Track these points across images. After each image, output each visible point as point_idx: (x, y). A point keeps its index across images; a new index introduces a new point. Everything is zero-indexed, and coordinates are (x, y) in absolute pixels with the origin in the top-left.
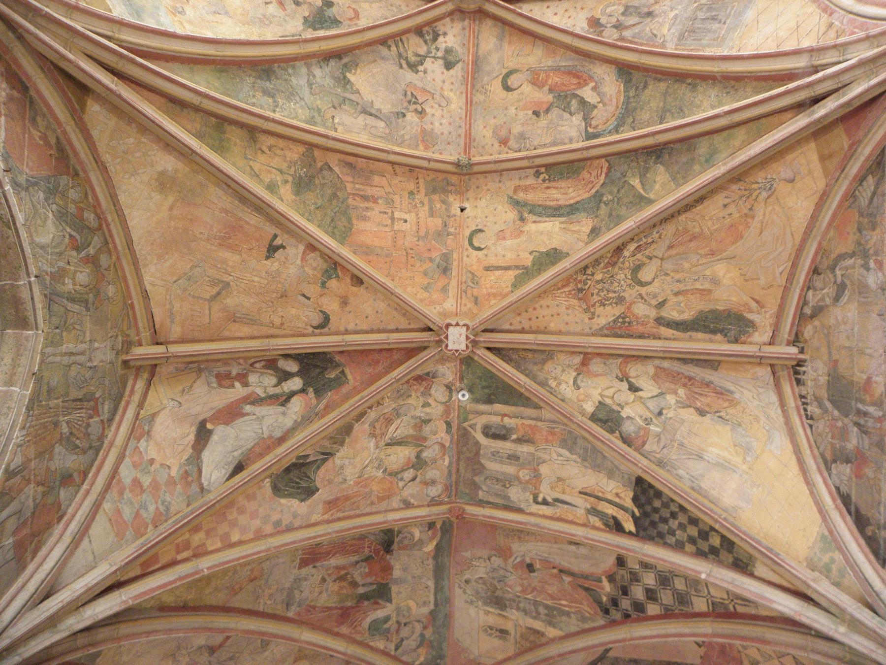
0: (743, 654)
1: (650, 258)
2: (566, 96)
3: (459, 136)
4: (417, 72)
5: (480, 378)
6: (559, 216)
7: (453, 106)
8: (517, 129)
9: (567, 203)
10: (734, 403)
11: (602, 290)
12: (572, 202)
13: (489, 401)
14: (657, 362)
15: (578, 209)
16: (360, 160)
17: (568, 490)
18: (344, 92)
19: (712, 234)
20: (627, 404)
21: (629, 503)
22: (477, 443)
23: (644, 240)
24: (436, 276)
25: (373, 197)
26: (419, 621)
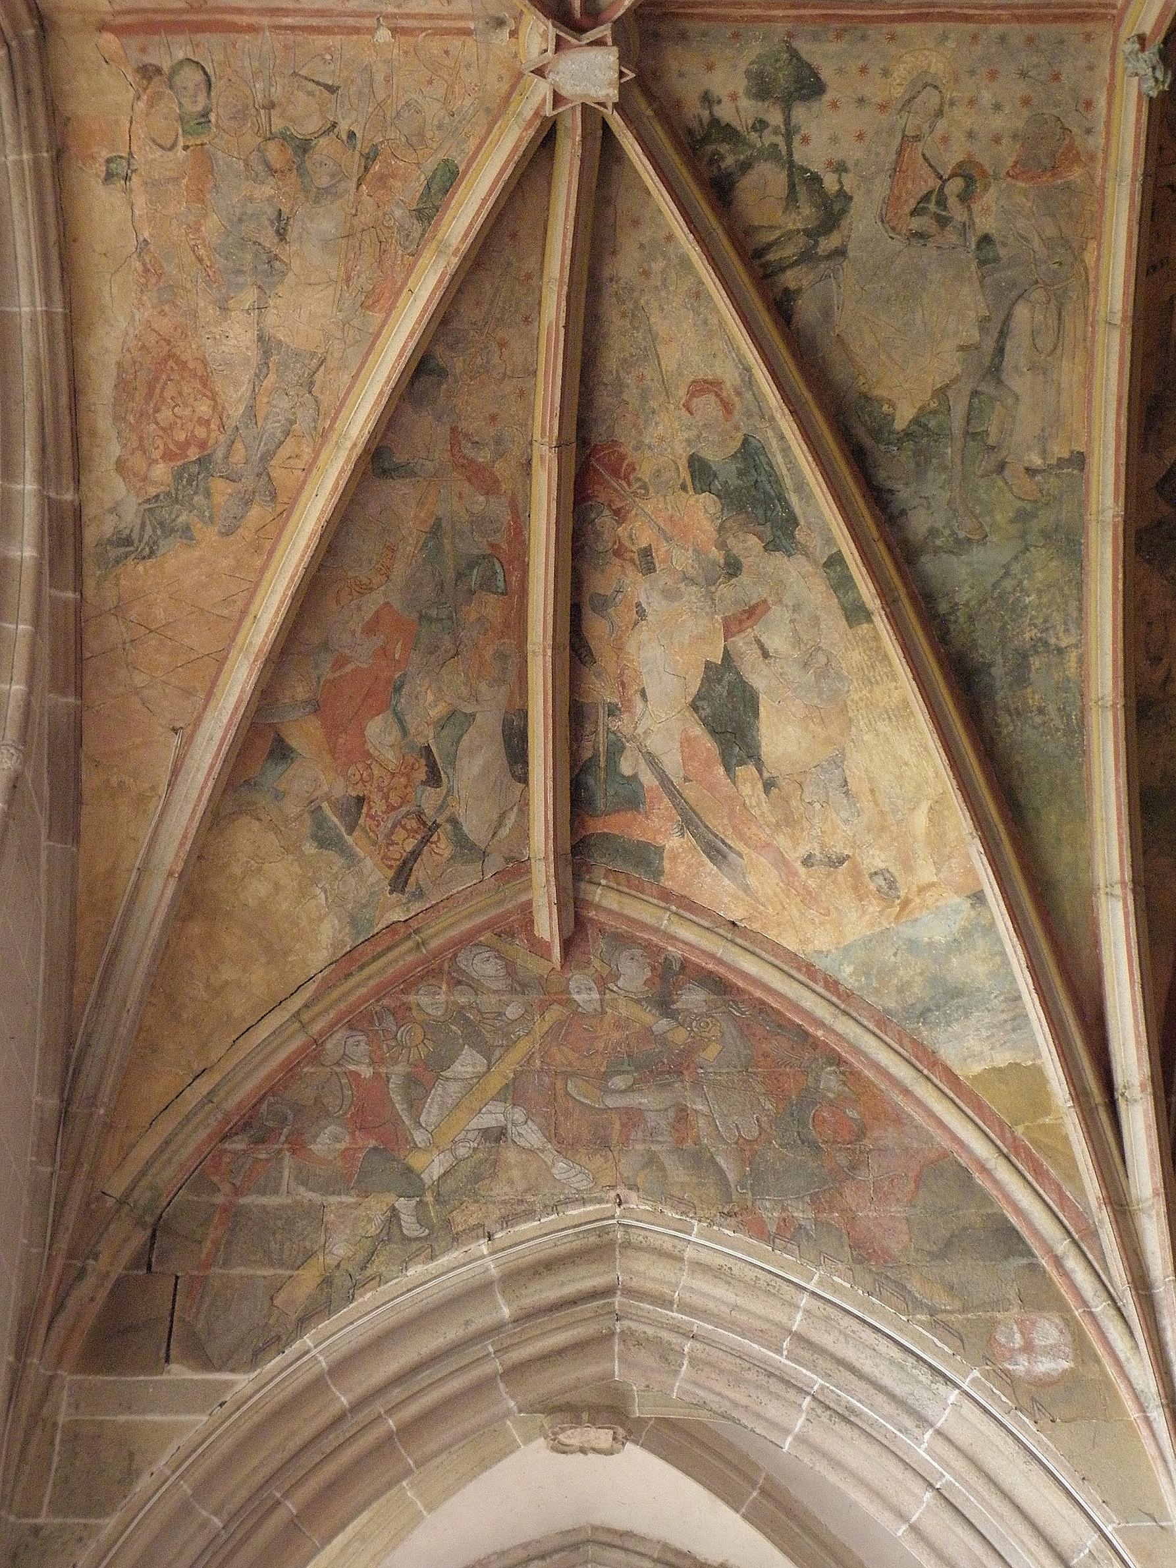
3: (1030, 40)
4: (845, 197)
7: (937, 65)
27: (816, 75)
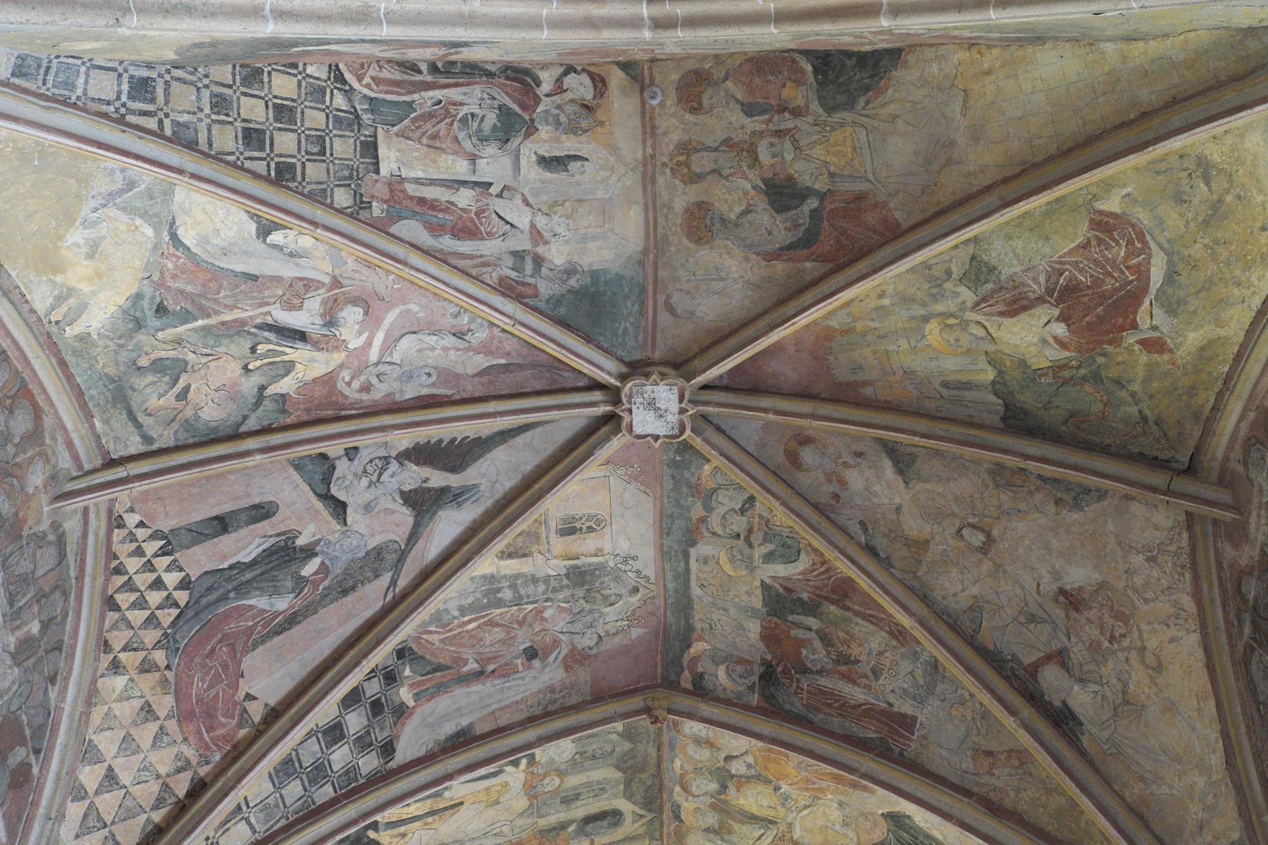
0: (179, 738)
17: (482, 796)
22: (629, 796)
26: (714, 534)
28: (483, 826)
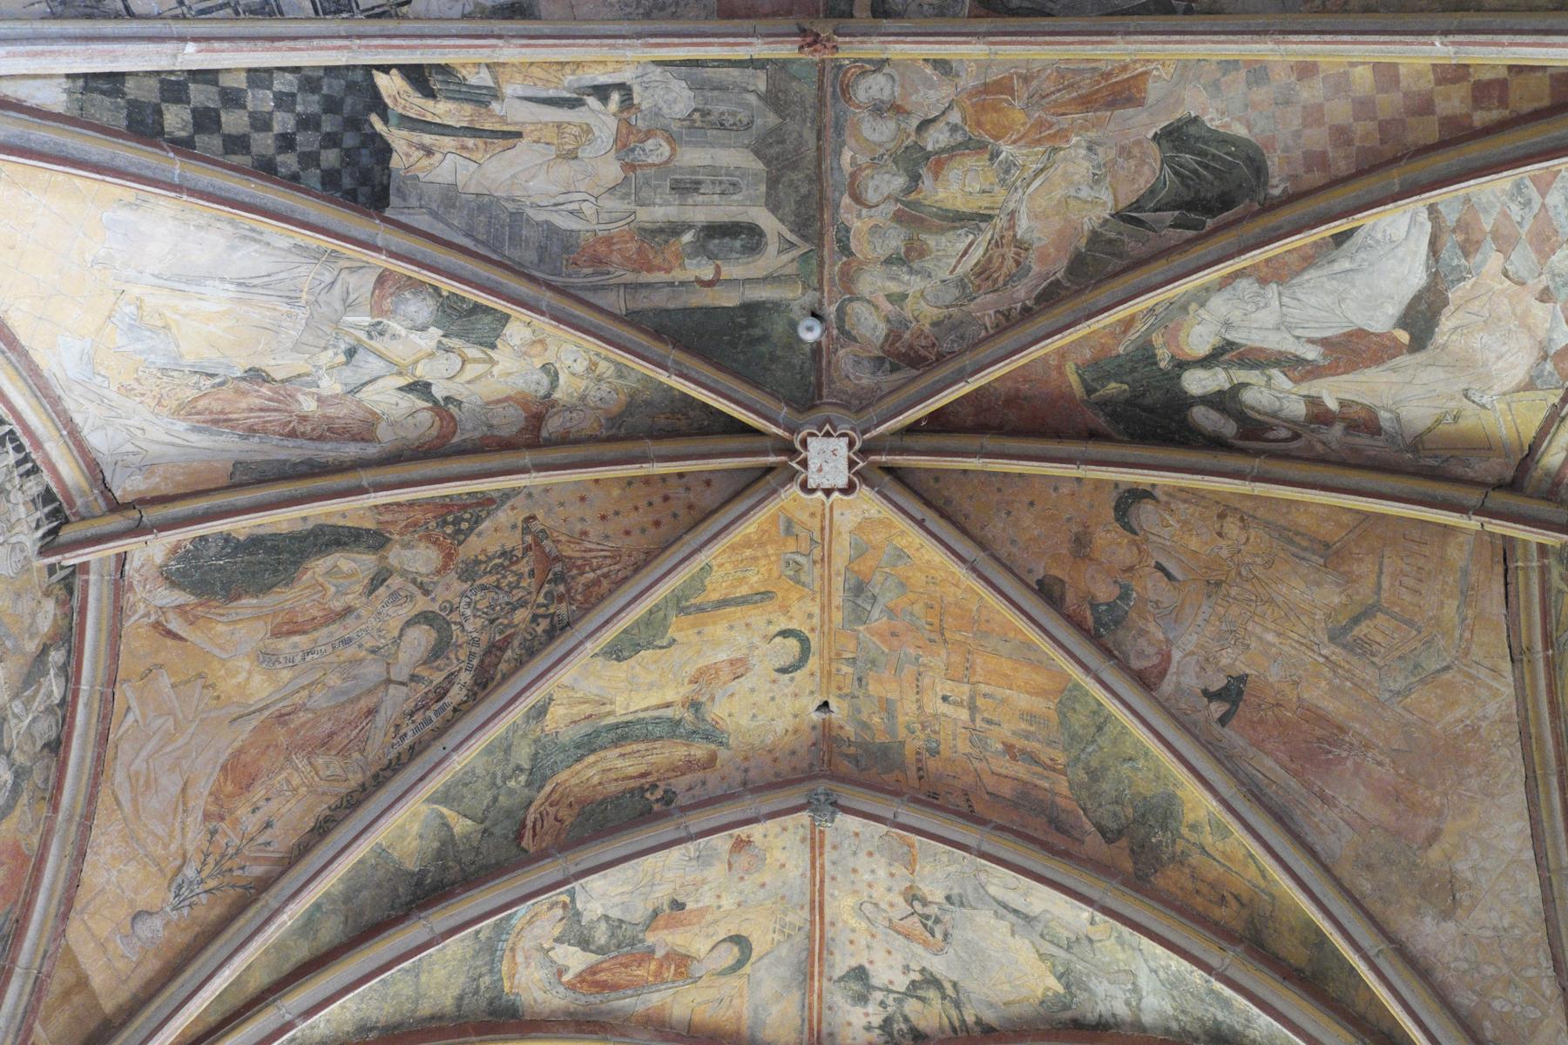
1: (414, 678)
2: (619, 946)
3: (834, 847)
4: (923, 970)
5: (773, 359)
6: (617, 726)
7: (850, 901)
8: (717, 871)
9: (602, 754)
10: (187, 410)
11: (513, 587)
12: (591, 758)
13: (751, 309)
14: (372, 450)
15: (577, 747)
16: (1039, 835)
17: (550, 134)
18: (1069, 962)
19: (288, 759)
20: (431, 355)
21: (398, 138)
22: (774, 207)
23: (430, 714)
24: (878, 578)
25: (1014, 758)
27: (853, 970)
28: (554, 189)
